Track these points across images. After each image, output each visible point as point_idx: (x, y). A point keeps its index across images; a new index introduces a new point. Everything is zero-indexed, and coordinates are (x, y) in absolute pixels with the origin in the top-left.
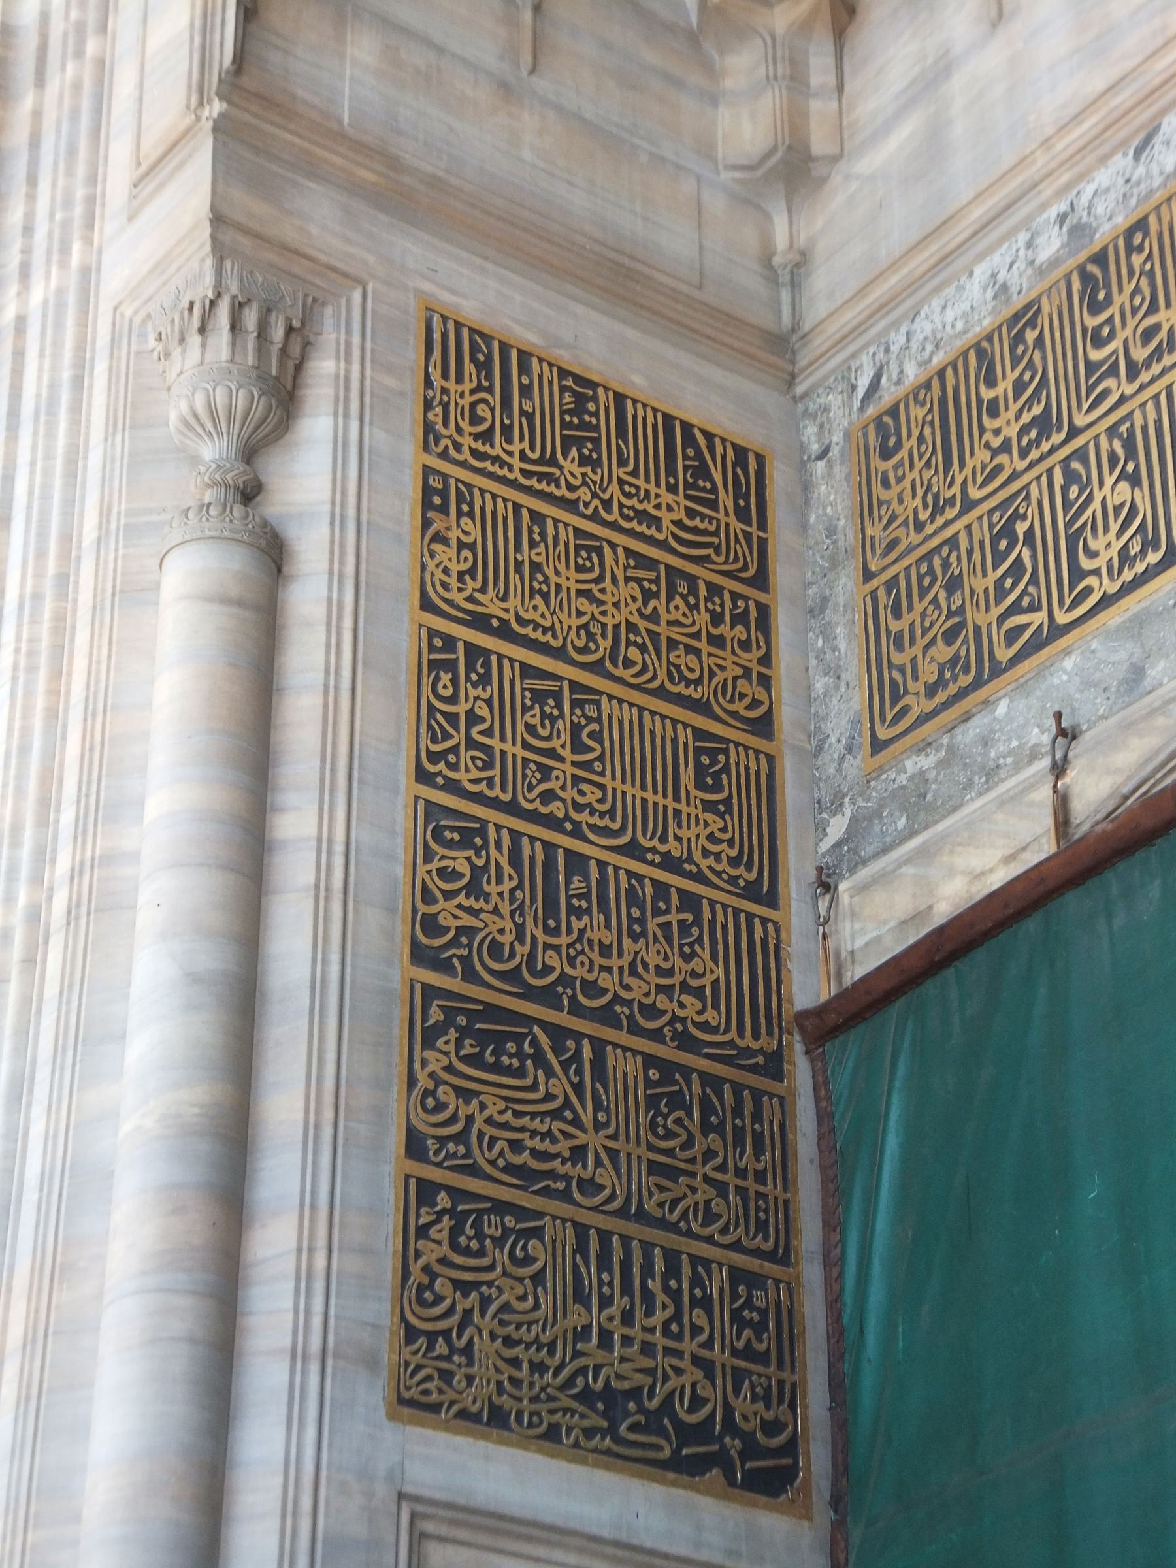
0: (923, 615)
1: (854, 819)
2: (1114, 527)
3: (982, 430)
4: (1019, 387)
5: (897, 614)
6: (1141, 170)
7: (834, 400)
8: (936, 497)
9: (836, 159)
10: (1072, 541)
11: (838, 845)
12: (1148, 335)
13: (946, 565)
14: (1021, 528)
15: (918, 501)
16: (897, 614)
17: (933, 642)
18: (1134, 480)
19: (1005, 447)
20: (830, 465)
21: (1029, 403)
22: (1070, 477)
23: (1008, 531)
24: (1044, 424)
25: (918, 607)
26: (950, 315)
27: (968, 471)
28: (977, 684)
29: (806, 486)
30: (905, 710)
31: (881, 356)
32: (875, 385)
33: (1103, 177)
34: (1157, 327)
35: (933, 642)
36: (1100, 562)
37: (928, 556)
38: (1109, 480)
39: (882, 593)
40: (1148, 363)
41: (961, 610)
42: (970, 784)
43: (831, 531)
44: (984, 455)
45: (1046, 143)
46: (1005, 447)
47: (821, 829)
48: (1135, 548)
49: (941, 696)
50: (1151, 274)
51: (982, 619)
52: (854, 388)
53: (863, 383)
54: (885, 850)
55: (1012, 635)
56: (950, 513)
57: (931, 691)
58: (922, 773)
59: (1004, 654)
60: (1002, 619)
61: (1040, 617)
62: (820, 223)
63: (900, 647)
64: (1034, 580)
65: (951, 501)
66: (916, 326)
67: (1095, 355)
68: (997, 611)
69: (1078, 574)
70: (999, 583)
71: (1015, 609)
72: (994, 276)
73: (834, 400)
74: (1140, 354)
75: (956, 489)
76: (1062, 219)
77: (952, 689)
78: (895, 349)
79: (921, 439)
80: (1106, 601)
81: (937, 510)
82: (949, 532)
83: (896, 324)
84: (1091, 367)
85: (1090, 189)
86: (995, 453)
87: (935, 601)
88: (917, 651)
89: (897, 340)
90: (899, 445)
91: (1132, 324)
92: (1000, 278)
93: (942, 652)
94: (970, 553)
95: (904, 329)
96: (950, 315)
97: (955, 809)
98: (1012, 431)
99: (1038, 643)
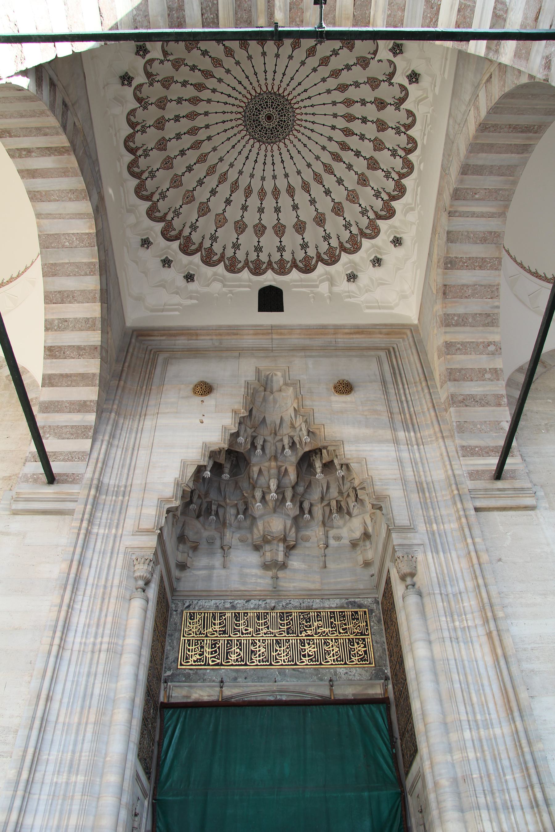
0: (195, 649)
1: (173, 674)
2: (236, 655)
3: (212, 626)
4: (220, 624)
5: (189, 645)
6: (246, 605)
7: (180, 604)
8: (201, 631)
9: (189, 568)
10: (227, 653)
11: (168, 676)
12: (246, 630)
13: (201, 643)
14: (217, 646)
15: (197, 630)
16: (189, 645)
17: (196, 654)
18: (241, 650)
19: (216, 631)
20: (177, 613)
21: (222, 627)
22: (228, 643)
23: (215, 644)
24: (224, 632)
25: (194, 647)
26: (206, 604)
27: (208, 631)
28: (205, 665)
29: (171, 614)
30: (189, 662)
31: (191, 602)
32: (188, 607)
33: (239, 601)
34: (248, 630)
35: (196, 654)
36: (233, 658)
37: (198, 640)
38: (236, 647)
39: (186, 641)
40: (246, 634)
41: (203, 652)
42: (199, 680)
43: (176, 624)
44: (211, 630)
45: (231, 591)
46: (216, 631)
47: (165, 672)
48: (239, 660)
49: (196, 663)
50: (248, 621)
51: (207, 655)
52: (184, 604)
53: (187, 605)
54: (179, 682)
55: (213, 661)
56: (203, 635)
57: (195, 661)
58: (189, 673)
59: (211, 663)
60: (211, 658)
61: (218, 661)
62: (183, 575)
63: (189, 651)
64: (219, 654)
65: (204, 634)
66: (199, 602)
67: (235, 627)
68: (210, 656)
69: (227, 658)
70: (212, 652)
71: (214, 657)
72: (216, 604)
73: (180, 604)
74: (244, 632)
75: (205, 632)
76: (231, 603)
77: (199, 663)
78: (194, 603)
79: (199, 621)
80: (232, 665)
81: (200, 633)
82: (203, 638)
83: (195, 600)
84: (235, 629)
85: (236, 602)
86: (214, 631)
87: (198, 648)
88: (193, 653)
89: (195, 602)
90: (194, 619)
91: (243, 626)
92: (218, 604)
93: (198, 657)
94: (206, 644)
95: (197, 601)
96: (206, 604)
97: (196, 682)
98: (218, 630)
99: (217, 665)
